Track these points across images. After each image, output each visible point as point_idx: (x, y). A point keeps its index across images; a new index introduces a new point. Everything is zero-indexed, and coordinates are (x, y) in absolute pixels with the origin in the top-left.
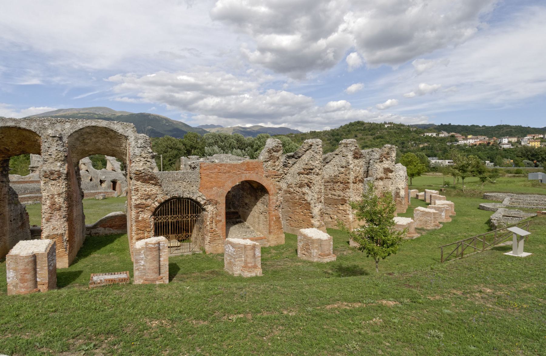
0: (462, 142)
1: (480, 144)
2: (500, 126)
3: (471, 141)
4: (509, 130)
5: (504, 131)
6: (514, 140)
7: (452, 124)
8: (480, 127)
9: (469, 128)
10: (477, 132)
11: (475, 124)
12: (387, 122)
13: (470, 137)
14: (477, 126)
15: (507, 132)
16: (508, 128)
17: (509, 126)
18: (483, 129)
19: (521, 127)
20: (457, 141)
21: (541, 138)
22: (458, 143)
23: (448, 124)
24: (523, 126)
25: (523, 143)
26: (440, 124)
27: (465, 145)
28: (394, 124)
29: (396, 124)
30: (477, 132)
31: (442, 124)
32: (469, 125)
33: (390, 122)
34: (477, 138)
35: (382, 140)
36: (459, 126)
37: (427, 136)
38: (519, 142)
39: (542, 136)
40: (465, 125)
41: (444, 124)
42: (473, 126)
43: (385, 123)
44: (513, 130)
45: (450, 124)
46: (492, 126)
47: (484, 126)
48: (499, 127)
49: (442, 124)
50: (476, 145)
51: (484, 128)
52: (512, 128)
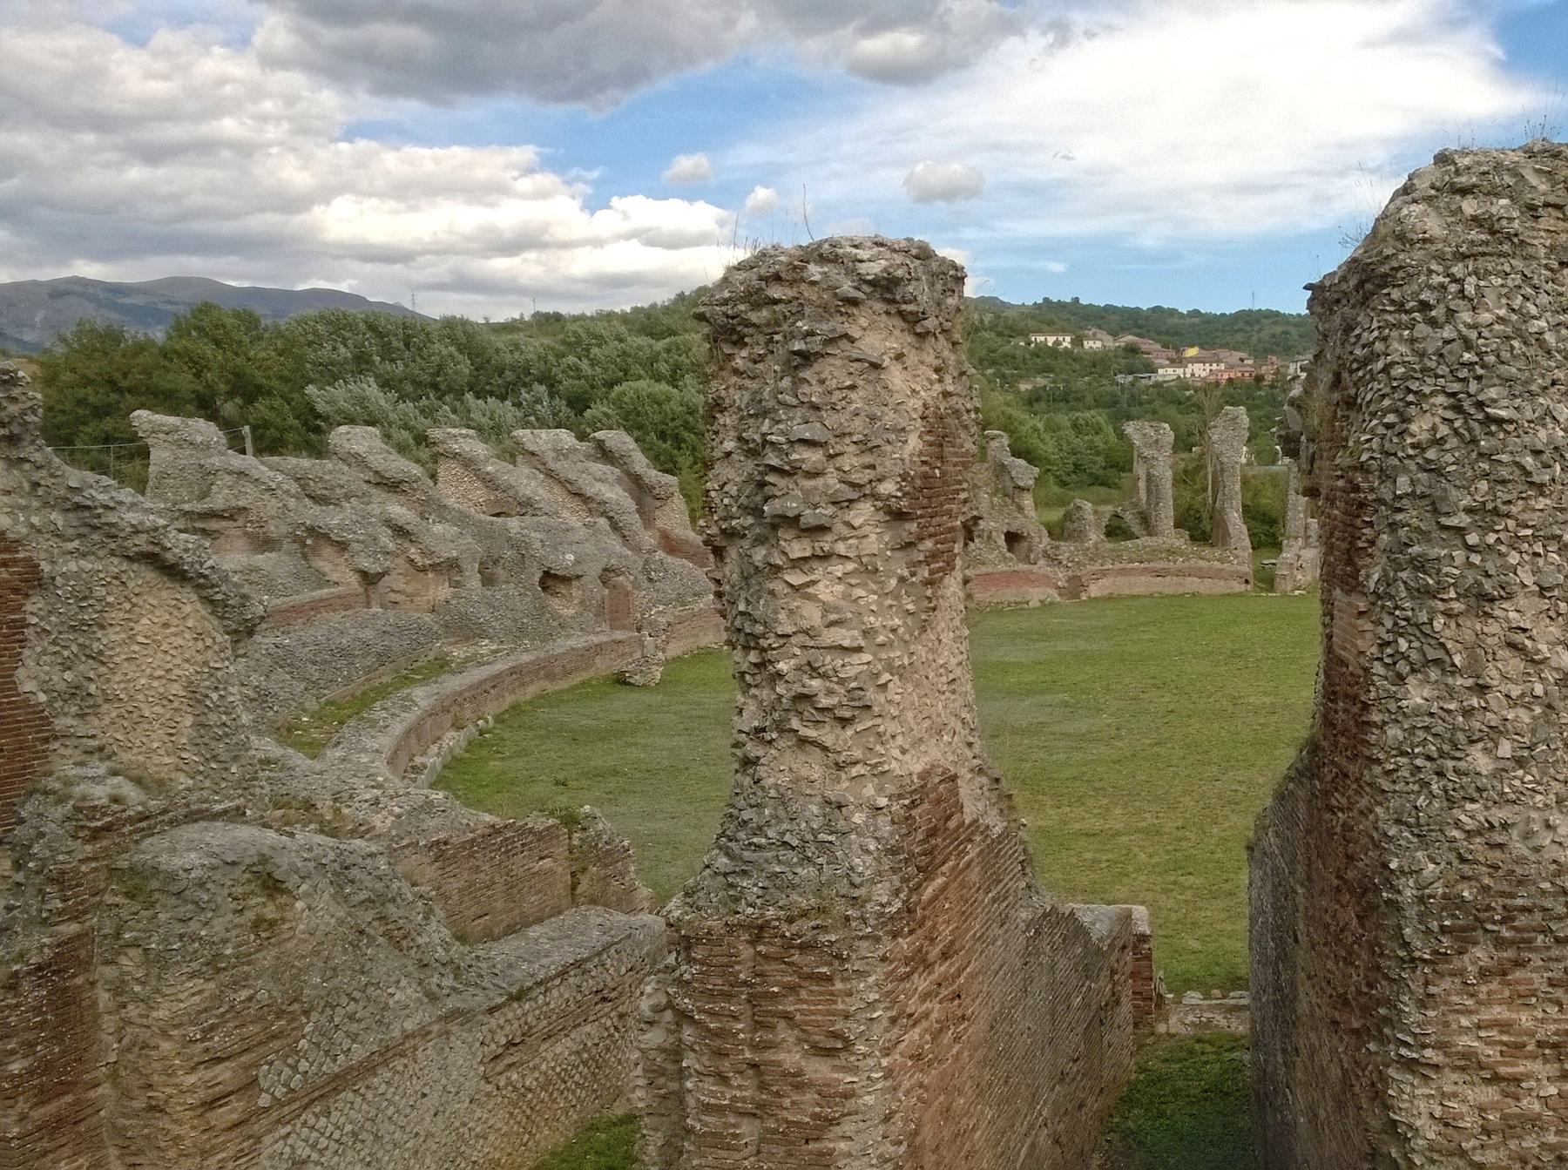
0: (1167, 373)
4: (1279, 329)
5: (1265, 334)
7: (1083, 302)
9: (1147, 319)
10: (1176, 334)
15: (1274, 336)
16: (1275, 323)
17: (1277, 314)
18: (1193, 325)
23: (1068, 300)
26: (1040, 301)
30: (1176, 334)
31: (1046, 300)
32: (1145, 306)
36: (1109, 309)
40: (1131, 304)
41: (1055, 300)
44: (1294, 331)
45: (1077, 299)
46: (1223, 315)
47: (1196, 313)
48: (1249, 319)
49: (1046, 300)
52: (1288, 323)
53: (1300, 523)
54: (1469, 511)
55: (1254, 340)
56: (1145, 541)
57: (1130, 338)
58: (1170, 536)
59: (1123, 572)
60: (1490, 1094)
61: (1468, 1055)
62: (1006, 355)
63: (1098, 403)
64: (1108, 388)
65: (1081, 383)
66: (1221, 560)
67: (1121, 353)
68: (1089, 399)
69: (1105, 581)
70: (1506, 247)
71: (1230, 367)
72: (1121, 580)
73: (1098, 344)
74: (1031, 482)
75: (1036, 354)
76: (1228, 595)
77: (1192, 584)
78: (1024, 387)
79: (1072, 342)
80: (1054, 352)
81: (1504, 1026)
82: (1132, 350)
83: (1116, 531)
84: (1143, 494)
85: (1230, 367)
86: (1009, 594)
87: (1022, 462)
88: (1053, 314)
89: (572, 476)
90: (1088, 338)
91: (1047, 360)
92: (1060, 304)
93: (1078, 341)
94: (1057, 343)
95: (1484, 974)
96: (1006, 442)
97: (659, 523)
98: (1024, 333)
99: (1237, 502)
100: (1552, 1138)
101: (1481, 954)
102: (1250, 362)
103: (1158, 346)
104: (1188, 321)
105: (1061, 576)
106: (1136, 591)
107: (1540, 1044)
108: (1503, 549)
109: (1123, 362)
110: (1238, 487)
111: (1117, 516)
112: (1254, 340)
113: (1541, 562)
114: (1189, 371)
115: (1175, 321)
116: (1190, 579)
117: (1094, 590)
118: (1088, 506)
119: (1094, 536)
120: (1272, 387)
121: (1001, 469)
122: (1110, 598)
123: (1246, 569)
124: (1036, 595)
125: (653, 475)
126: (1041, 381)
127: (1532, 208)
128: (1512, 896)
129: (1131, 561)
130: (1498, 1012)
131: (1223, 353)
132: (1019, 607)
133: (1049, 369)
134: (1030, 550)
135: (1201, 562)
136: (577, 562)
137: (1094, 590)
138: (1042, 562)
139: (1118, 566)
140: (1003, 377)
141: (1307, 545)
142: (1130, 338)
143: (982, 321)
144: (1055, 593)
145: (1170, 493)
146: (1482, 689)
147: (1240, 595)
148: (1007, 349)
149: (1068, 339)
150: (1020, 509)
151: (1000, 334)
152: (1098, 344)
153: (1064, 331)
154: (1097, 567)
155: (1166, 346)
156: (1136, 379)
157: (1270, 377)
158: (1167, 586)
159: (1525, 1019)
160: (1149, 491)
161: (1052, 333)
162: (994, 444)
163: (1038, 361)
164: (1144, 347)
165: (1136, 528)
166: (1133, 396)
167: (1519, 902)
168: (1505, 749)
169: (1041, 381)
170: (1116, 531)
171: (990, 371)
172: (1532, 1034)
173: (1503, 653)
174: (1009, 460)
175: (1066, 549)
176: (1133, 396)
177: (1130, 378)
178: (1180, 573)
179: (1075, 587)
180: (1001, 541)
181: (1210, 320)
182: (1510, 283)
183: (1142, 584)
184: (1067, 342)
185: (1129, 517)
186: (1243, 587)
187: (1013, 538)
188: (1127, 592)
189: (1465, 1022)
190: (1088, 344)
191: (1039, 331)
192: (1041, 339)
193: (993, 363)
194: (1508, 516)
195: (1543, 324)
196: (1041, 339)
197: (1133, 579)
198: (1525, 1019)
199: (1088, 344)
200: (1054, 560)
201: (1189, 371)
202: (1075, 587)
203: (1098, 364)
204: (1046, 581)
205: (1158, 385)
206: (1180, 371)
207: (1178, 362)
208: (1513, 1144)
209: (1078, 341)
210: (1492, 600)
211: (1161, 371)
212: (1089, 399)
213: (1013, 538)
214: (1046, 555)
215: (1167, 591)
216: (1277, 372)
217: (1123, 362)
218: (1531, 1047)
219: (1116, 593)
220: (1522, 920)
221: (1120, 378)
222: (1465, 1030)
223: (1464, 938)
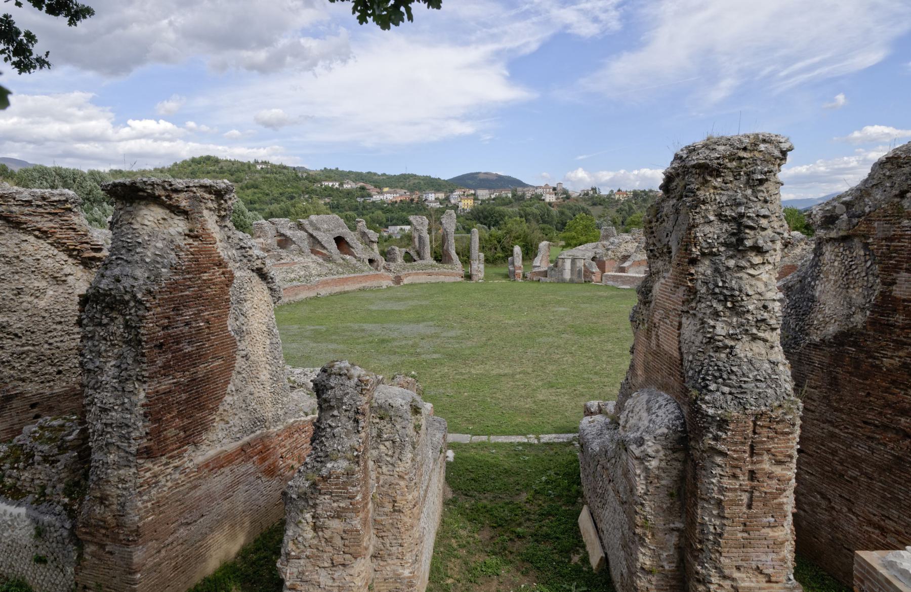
1: (401, 201)
2: (404, 175)
3: (389, 196)
4: (416, 181)
5: (411, 183)
6: (441, 196)
7: (340, 169)
8: (379, 175)
11: (373, 171)
12: (260, 162)
13: (386, 189)
14: (375, 174)
15: (414, 184)
17: (415, 175)
18: (383, 179)
19: (430, 177)
20: (370, 196)
21: (472, 194)
22: (372, 199)
24: (433, 176)
25: (453, 201)
27: (383, 202)
28: (272, 165)
29: (275, 165)
31: (325, 168)
32: (364, 172)
33: (264, 160)
34: (396, 193)
35: (256, 190)
36: (350, 172)
37: (326, 188)
38: (447, 199)
39: (473, 192)
40: (359, 171)
42: (369, 173)
43: (256, 162)
44: (422, 182)
45: (337, 169)
47: (384, 175)
49: (325, 168)
50: (396, 202)
51: (385, 177)
53: (477, 255)
55: (407, 185)
56: (420, 262)
57: (362, 184)
58: (429, 260)
59: (417, 274)
62: (312, 190)
63: (350, 209)
64: (354, 203)
65: (343, 201)
68: (347, 207)
71: (401, 195)
72: (415, 277)
73: (349, 186)
74: (377, 239)
76: (455, 282)
77: (442, 278)
80: (332, 189)
82: (363, 188)
83: (408, 258)
84: (417, 243)
85: (401, 195)
86: (375, 283)
87: (371, 231)
88: (329, 174)
91: (329, 192)
92: (331, 170)
93: (341, 184)
94: (333, 185)
96: (364, 223)
98: (320, 181)
99: (454, 247)
102: (408, 194)
103: (373, 187)
104: (381, 178)
105: (391, 275)
106: (421, 282)
109: (359, 193)
110: (453, 241)
111: (407, 252)
112: (407, 185)
114: (385, 197)
115: (376, 177)
117: (406, 281)
118: (397, 248)
119: (400, 260)
120: (417, 203)
121: (364, 234)
122: (412, 284)
123: (461, 272)
124: (385, 283)
129: (418, 270)
131: (398, 190)
132: (379, 289)
133: (330, 196)
134: (378, 266)
135: (445, 270)
137: (406, 281)
138: (383, 270)
139: (414, 272)
141: (479, 263)
142: (362, 184)
144: (391, 282)
148: (314, 187)
149: (337, 184)
150: (373, 250)
151: (310, 182)
152: (349, 186)
153: (335, 181)
154: (406, 272)
155: (376, 187)
157: (416, 200)
158: (433, 279)
160: (420, 242)
161: (332, 181)
162: (360, 224)
164: (367, 187)
165: (416, 257)
166: (364, 207)
170: (408, 258)
171: (307, 196)
174: (367, 231)
175: (392, 266)
176: (364, 207)
177: (362, 199)
178: (437, 274)
179: (398, 280)
180: (368, 263)
181: (390, 177)
183: (423, 279)
184: (337, 185)
185: (412, 253)
187: (371, 261)
188: (417, 282)
190: (345, 186)
191: (325, 181)
192: (326, 184)
193: (308, 193)
196: (326, 184)
197: (420, 277)
199: (345, 186)
200: (388, 269)
201: (385, 197)
202: (398, 280)
203: (349, 193)
204: (387, 278)
205: (374, 202)
206: (382, 197)
207: (381, 193)
209: (341, 184)
211: (374, 197)
212: (347, 207)
213: (371, 261)
214: (384, 268)
215: (433, 281)
216: (419, 198)
217: (359, 193)
221: (358, 199)
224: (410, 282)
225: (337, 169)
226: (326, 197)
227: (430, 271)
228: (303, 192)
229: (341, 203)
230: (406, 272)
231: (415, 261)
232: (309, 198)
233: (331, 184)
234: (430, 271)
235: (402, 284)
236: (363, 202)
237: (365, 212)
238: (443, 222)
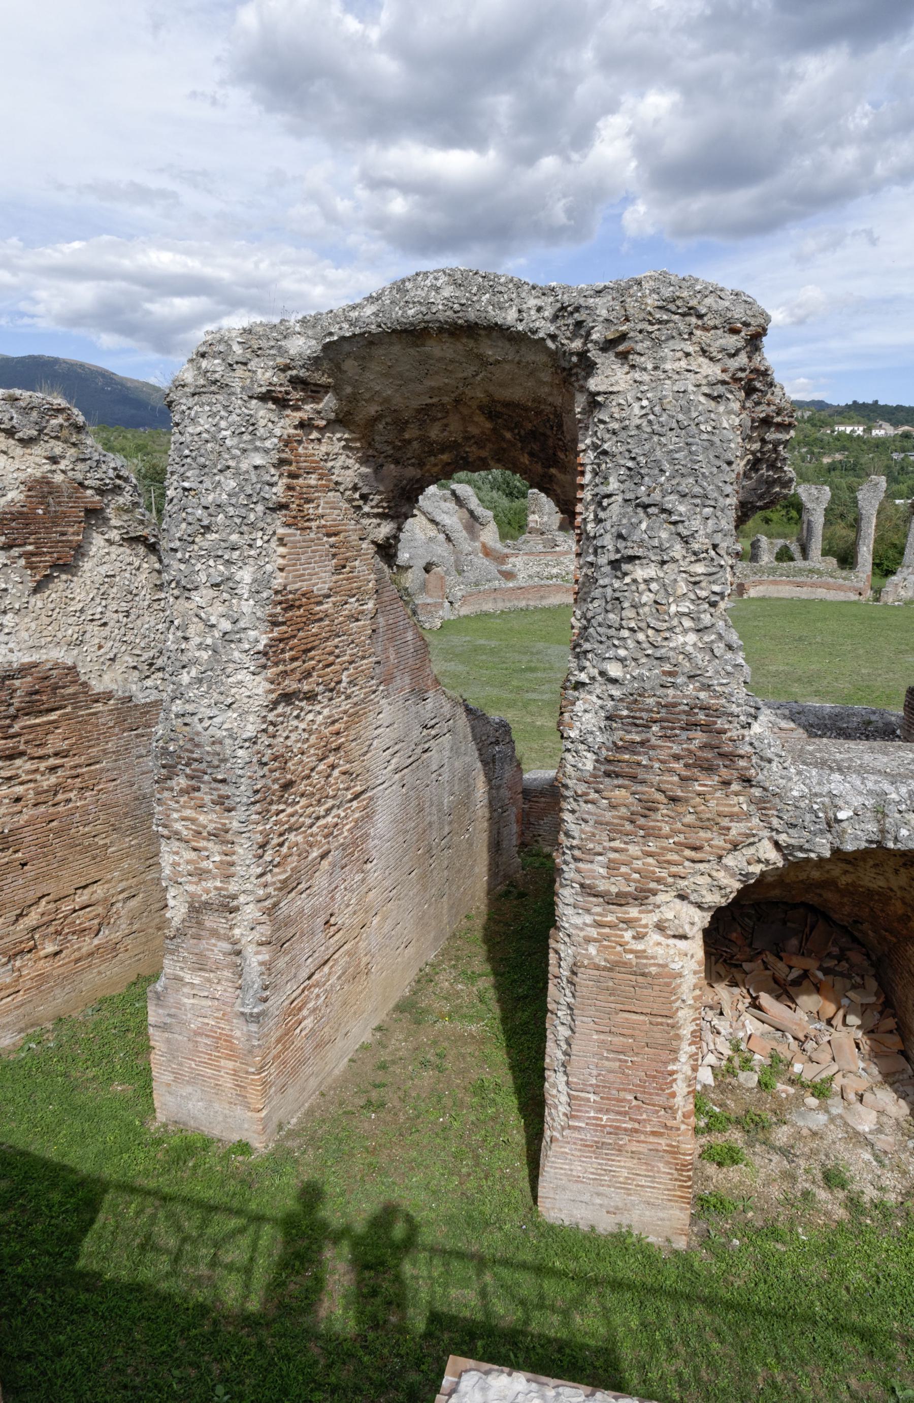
7: (881, 403)
23: (870, 402)
26: (850, 403)
31: (855, 402)
36: (899, 408)
41: (861, 402)
45: (876, 402)
49: (855, 402)
54: (180, 540)
59: (775, 583)
60: (193, 855)
61: (177, 833)
62: (817, 439)
66: (844, 579)
67: (898, 439)
69: (761, 588)
70: (213, 388)
75: (837, 439)
78: (826, 460)
79: (864, 431)
80: (850, 437)
81: (193, 821)
83: (784, 555)
89: (430, 510)
90: (875, 428)
93: (868, 430)
94: (853, 431)
95: (183, 792)
97: (482, 539)
98: (831, 425)
100: (218, 884)
101: (181, 782)
106: (781, 595)
107: (210, 834)
108: (193, 561)
113: (212, 570)
116: (820, 590)
117: (753, 593)
125: (480, 511)
126: (838, 457)
127: (231, 365)
128: (192, 752)
129: (781, 575)
130: (188, 813)
133: (844, 448)
136: (411, 558)
137: (753, 593)
139: (771, 578)
140: (812, 453)
142: (906, 428)
143: (803, 417)
145: (820, 533)
146: (186, 639)
147: (855, 603)
148: (818, 435)
149: (861, 428)
151: (814, 425)
156: (906, 456)
158: (804, 593)
159: (202, 819)
163: (838, 443)
166: (902, 468)
167: (195, 756)
168: (194, 673)
169: (838, 457)
170: (784, 555)
171: (804, 450)
172: (205, 827)
173: (196, 620)
177: (902, 455)
178: (813, 585)
182: (214, 410)
184: (860, 430)
186: (856, 598)
188: (775, 595)
189: (175, 815)
190: (876, 432)
192: (842, 428)
193: (807, 444)
194: (193, 542)
195: (227, 433)
196: (842, 428)
197: (780, 587)
198: (202, 819)
203: (880, 445)
208: (204, 883)
209: (868, 430)
210: (189, 590)
215: (804, 596)
217: (898, 444)
218: (205, 834)
219: (767, 595)
220: (195, 765)
221: (895, 456)
222: (176, 820)
223: (171, 771)
224: (761, 594)
225: (876, 402)
226: (838, 451)
227: (802, 579)
228: (799, 443)
229: (863, 461)
230: (757, 578)
231: (792, 559)
232: (807, 452)
233: (849, 430)
234: (802, 579)
235: (745, 596)
236: (903, 459)
237: (901, 478)
238: (860, 497)
